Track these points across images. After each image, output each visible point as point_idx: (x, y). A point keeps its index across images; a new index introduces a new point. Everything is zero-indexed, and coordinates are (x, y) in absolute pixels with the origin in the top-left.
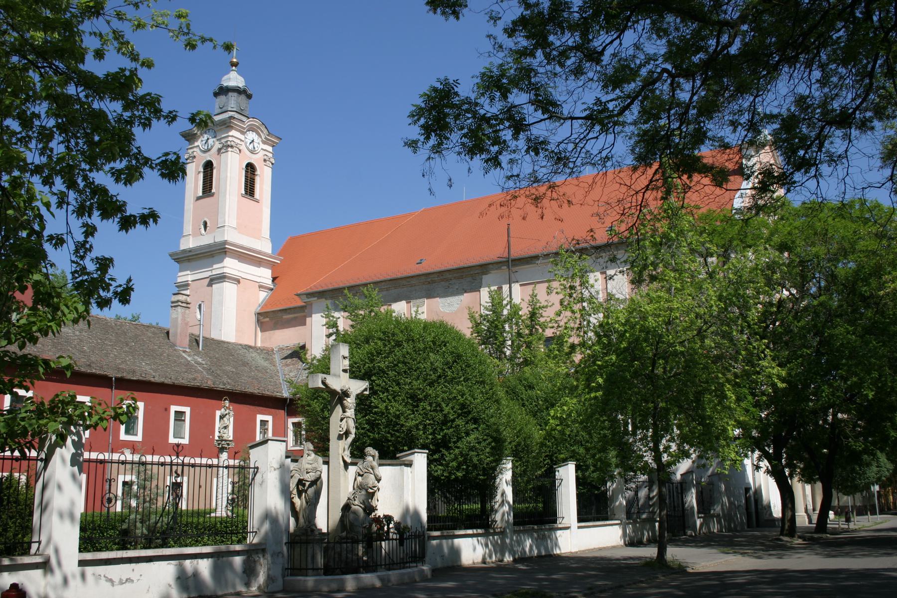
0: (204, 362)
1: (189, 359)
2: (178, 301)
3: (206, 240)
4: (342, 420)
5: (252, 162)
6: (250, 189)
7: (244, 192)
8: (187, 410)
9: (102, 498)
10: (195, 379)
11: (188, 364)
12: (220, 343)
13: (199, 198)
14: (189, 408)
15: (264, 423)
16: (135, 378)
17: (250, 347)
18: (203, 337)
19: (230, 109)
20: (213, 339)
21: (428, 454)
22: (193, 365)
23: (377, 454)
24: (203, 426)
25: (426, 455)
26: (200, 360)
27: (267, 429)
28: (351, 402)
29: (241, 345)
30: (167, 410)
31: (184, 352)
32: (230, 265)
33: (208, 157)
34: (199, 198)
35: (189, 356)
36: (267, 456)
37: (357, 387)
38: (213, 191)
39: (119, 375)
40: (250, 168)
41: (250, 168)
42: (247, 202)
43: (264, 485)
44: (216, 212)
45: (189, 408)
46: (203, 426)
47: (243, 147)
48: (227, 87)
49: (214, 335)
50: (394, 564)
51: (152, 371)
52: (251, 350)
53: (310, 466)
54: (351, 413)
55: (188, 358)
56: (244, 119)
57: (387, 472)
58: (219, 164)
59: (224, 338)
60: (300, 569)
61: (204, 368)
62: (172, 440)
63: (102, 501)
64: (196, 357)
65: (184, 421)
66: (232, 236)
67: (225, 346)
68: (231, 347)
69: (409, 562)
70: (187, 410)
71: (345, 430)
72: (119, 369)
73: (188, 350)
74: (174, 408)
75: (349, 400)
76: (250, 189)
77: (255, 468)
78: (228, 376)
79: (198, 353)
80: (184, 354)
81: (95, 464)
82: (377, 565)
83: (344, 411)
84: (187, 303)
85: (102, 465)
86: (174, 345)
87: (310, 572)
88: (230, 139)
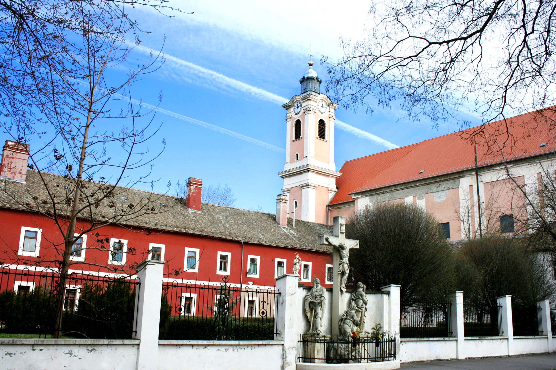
0: (295, 234)
1: (287, 232)
2: (280, 199)
3: (297, 165)
4: (340, 264)
5: (322, 119)
6: (322, 134)
7: (318, 137)
8: (229, 254)
9: (176, 308)
10: (289, 243)
11: (286, 235)
12: (305, 223)
13: (294, 141)
14: (127, 241)
15: (223, 258)
16: (255, 243)
17: (324, 225)
18: (295, 219)
19: (309, 90)
20: (302, 221)
21: (400, 287)
22: (289, 236)
23: (365, 286)
24: (239, 264)
25: (399, 288)
26: (293, 232)
27: (309, 270)
28: (346, 252)
29: (318, 224)
30: (273, 261)
31: (284, 228)
32: (311, 178)
33: (297, 117)
34: (294, 141)
35: (287, 230)
36: (285, 285)
37: (352, 244)
38: (301, 137)
39: (246, 241)
40: (322, 123)
41: (322, 123)
42: (321, 141)
43: (284, 304)
44: (302, 149)
45: (127, 241)
46: (239, 264)
47: (317, 111)
48: (307, 77)
49: (304, 219)
50: (307, 358)
51: (264, 239)
52: (324, 227)
53: (317, 293)
54: (346, 260)
55: (286, 231)
56: (317, 94)
57: (371, 299)
58: (304, 121)
59: (309, 220)
60: (311, 359)
61: (295, 237)
62: (219, 272)
63: (176, 310)
64: (291, 231)
65: (283, 267)
66: (312, 162)
67: (309, 224)
68: (312, 225)
69: (388, 357)
70: (229, 254)
71: (342, 271)
72: (245, 238)
73: (286, 227)
74: (220, 253)
75: (344, 252)
76: (322, 134)
77: (278, 293)
78: (309, 241)
79: (292, 229)
80: (284, 229)
81: (39, 277)
82: (361, 359)
83: (341, 259)
84: (286, 200)
85: (45, 278)
86: (279, 224)
87: (350, 361)
88: (309, 106)
